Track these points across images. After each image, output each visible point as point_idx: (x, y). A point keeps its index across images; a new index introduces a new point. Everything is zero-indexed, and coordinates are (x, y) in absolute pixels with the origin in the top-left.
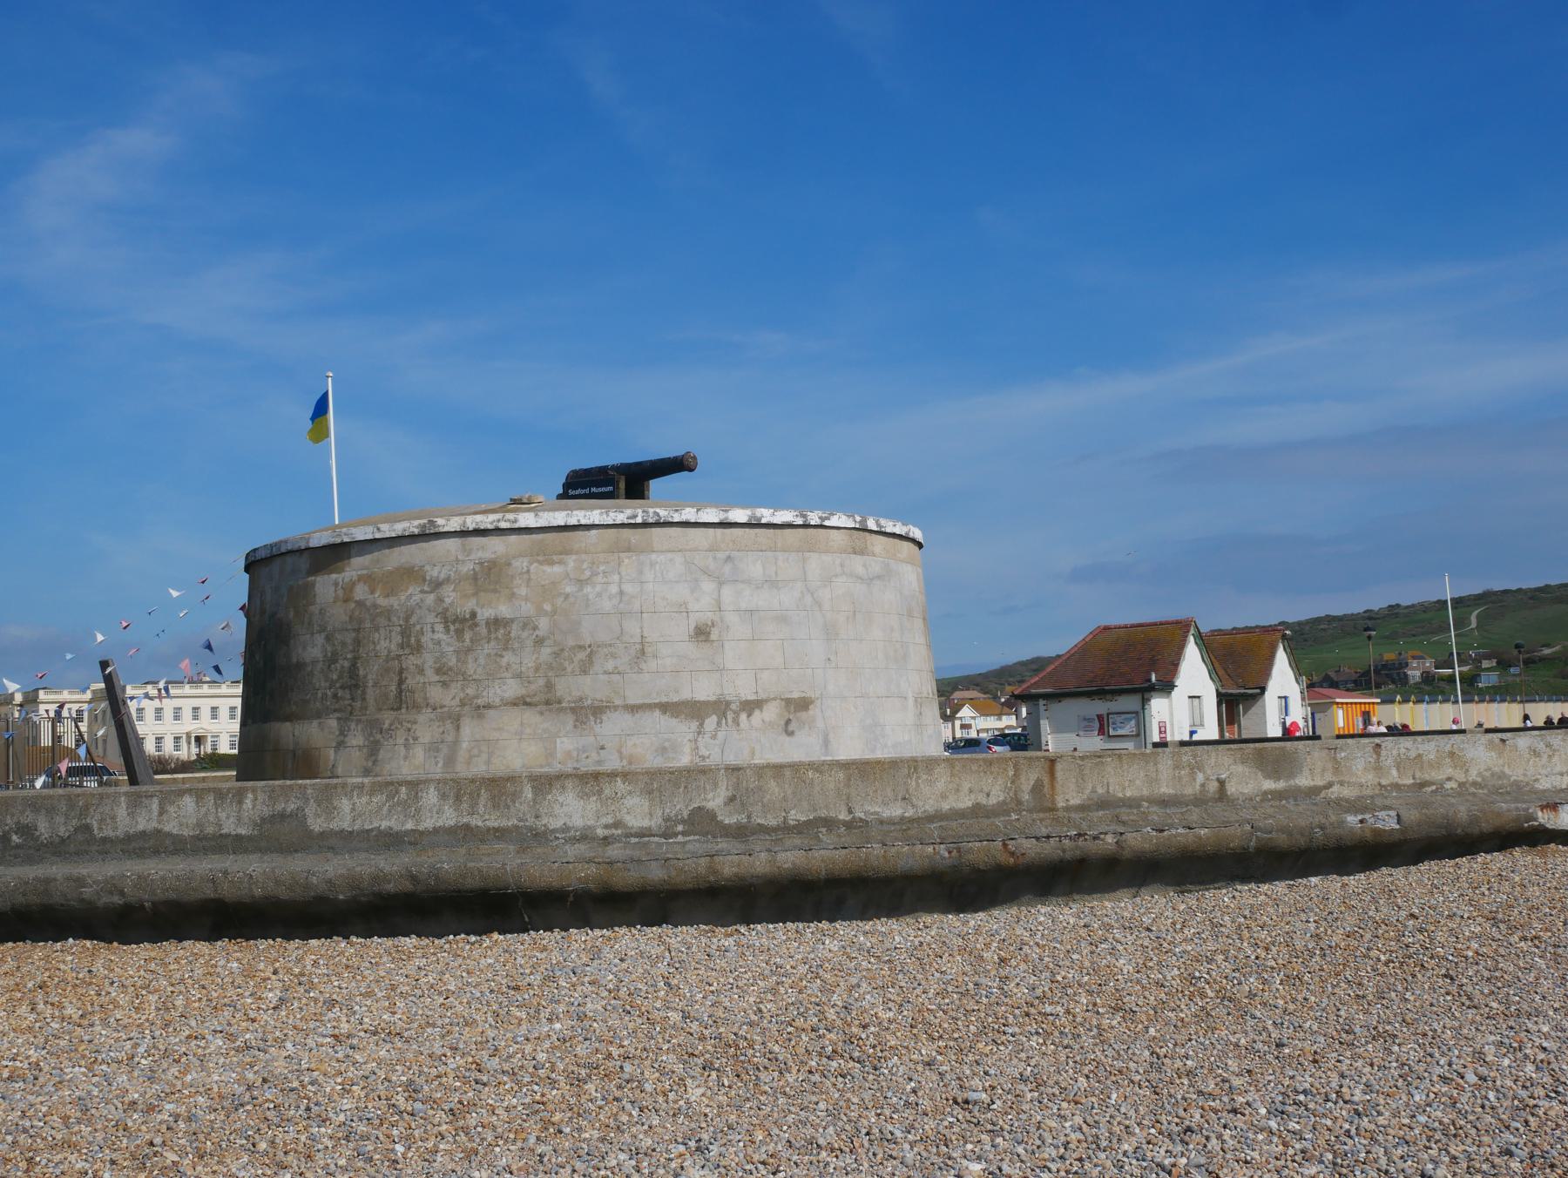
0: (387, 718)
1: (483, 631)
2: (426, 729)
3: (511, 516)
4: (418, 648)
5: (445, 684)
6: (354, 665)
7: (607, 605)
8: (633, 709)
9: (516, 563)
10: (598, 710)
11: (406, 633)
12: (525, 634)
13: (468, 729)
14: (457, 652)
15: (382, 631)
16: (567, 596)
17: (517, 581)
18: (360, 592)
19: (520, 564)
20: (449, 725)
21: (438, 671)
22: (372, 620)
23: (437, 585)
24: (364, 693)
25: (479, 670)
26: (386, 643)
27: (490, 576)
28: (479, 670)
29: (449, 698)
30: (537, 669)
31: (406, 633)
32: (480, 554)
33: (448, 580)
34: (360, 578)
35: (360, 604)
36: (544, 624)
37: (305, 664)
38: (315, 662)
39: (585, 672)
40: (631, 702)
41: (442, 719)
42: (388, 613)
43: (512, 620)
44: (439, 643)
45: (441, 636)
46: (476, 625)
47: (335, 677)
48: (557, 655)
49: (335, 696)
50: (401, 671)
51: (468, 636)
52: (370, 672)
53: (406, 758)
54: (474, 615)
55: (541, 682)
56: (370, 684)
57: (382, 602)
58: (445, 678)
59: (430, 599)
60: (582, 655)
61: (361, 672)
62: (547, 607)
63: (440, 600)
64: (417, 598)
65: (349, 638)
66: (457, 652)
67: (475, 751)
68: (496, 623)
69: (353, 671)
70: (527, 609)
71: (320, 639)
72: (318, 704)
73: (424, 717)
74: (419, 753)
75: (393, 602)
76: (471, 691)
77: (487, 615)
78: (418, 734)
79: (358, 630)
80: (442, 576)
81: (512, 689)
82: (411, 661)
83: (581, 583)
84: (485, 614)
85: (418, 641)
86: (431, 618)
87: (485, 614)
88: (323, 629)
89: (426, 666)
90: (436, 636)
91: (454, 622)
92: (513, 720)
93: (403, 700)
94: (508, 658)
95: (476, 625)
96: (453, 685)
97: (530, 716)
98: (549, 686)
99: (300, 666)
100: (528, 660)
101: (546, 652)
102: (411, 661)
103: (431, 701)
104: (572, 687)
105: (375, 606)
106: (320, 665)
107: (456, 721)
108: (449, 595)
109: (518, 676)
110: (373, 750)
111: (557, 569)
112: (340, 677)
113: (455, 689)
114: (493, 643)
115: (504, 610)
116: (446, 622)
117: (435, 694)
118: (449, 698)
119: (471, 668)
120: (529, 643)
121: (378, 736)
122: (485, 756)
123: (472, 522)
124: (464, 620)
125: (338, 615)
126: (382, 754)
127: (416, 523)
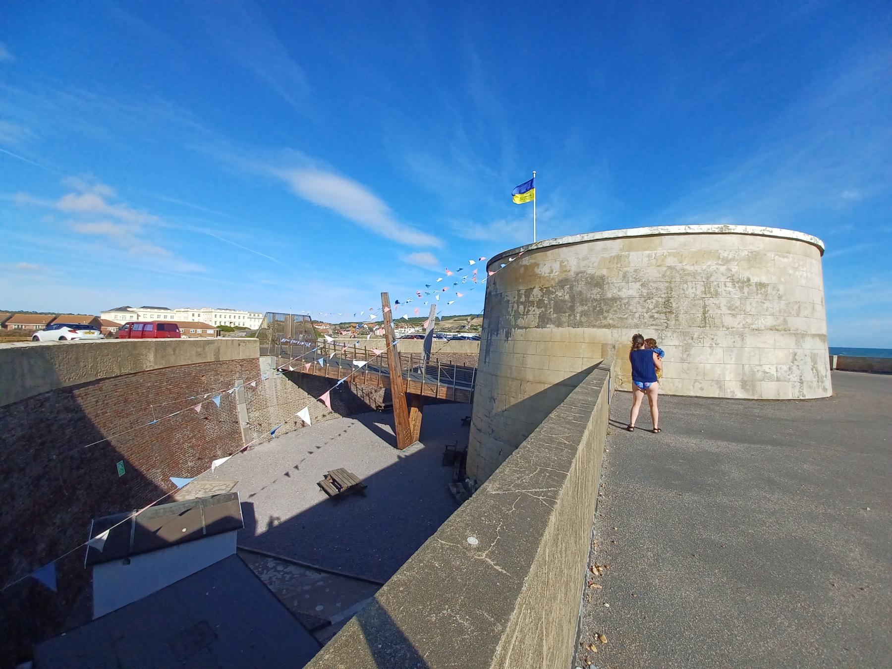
0: (696, 332)
1: (755, 289)
2: (724, 340)
3: (768, 229)
4: (717, 294)
5: (733, 315)
6: (667, 303)
7: (804, 282)
8: (814, 336)
9: (769, 254)
10: (803, 336)
11: (707, 285)
12: (774, 293)
13: (750, 341)
14: (740, 299)
15: (690, 284)
16: (790, 275)
17: (770, 265)
18: (670, 261)
19: (771, 255)
20: (737, 338)
21: (729, 308)
22: (681, 278)
23: (727, 261)
24: (677, 316)
25: (753, 309)
26: (694, 290)
27: (755, 258)
28: (753, 309)
29: (736, 323)
30: (780, 312)
31: (707, 285)
32: (751, 247)
33: (734, 259)
34: (670, 255)
35: (669, 267)
36: (781, 287)
37: (620, 299)
38: (630, 298)
39: (798, 316)
40: (814, 333)
41: (733, 334)
42: (694, 274)
43: (768, 285)
44: (730, 293)
45: (731, 289)
46: (750, 285)
47: (651, 307)
48: (787, 305)
49: (652, 317)
50: (705, 307)
51: (746, 290)
52: (681, 305)
53: (710, 355)
54: (749, 280)
55: (782, 319)
56: (682, 311)
57: (688, 267)
58: (733, 312)
59: (723, 269)
60: (796, 307)
61: (674, 305)
62: (783, 280)
63: (729, 270)
64: (715, 267)
65: (663, 286)
66: (740, 299)
67: (752, 354)
68: (761, 285)
69: (667, 303)
70: (774, 279)
71: (637, 285)
72: (635, 320)
73: (721, 333)
74: (719, 351)
75: (698, 268)
76: (749, 320)
77: (755, 280)
78: (718, 341)
79: (670, 282)
80: (730, 257)
81: (770, 321)
82: (711, 302)
83: (796, 269)
84: (754, 280)
85: (717, 291)
86: (723, 279)
87: (754, 280)
88: (636, 280)
89: (722, 305)
90: (727, 289)
91: (738, 282)
92: (770, 338)
93: (705, 320)
94: (767, 304)
95: (750, 285)
96: (739, 316)
97: (777, 336)
98: (785, 321)
99: (614, 299)
100: (775, 306)
101: (783, 302)
102: (711, 302)
103: (726, 324)
104: (796, 323)
105: (684, 270)
106: (637, 299)
107: (742, 336)
108: (734, 268)
109: (772, 314)
110: (687, 348)
111: (786, 260)
112: (656, 306)
113: (740, 318)
114: (759, 296)
115: (764, 279)
116: (733, 281)
117: (728, 320)
118: (736, 323)
119: (748, 308)
120: (776, 297)
121: (690, 341)
122: (758, 356)
123: (750, 229)
124: (743, 282)
125: (653, 273)
126: (693, 351)
127: (716, 226)
